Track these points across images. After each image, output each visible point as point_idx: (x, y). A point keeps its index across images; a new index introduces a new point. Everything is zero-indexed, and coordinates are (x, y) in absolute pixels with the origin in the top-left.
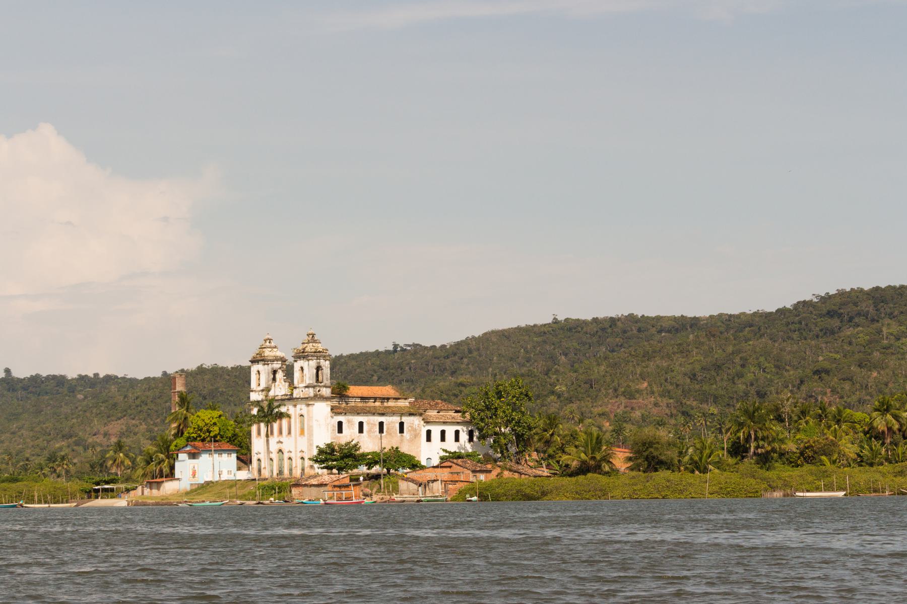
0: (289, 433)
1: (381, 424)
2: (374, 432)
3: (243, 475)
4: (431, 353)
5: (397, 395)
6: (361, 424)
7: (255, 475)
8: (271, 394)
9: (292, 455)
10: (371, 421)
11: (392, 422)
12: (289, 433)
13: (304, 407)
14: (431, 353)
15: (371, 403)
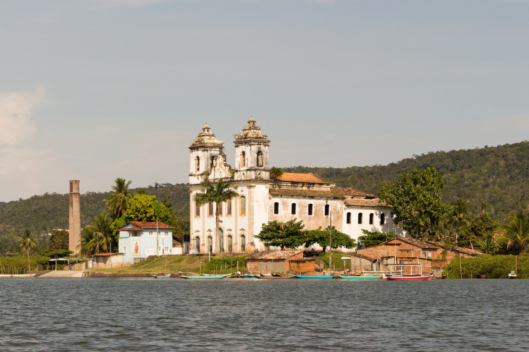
0: (230, 212)
1: (310, 206)
2: (305, 213)
3: (178, 251)
4: (182, 188)
5: (320, 181)
6: (294, 205)
7: (193, 251)
8: (211, 177)
9: (232, 233)
10: (302, 203)
11: (319, 204)
12: (230, 212)
13: (245, 189)
14: (182, 188)
15: (299, 188)
